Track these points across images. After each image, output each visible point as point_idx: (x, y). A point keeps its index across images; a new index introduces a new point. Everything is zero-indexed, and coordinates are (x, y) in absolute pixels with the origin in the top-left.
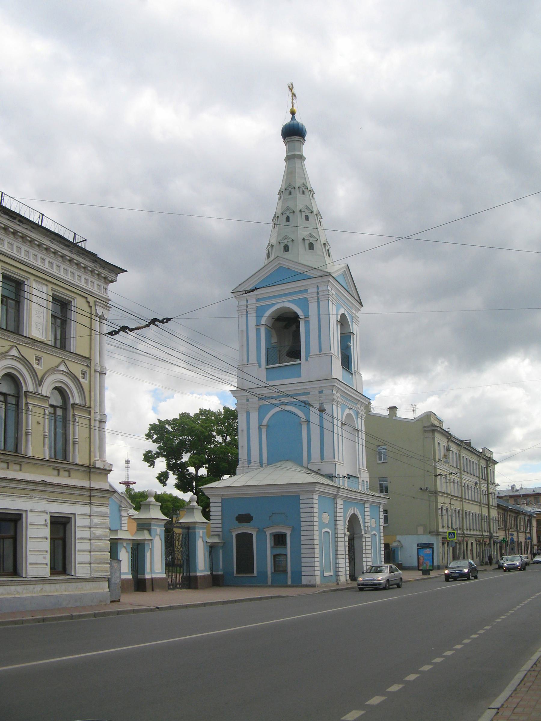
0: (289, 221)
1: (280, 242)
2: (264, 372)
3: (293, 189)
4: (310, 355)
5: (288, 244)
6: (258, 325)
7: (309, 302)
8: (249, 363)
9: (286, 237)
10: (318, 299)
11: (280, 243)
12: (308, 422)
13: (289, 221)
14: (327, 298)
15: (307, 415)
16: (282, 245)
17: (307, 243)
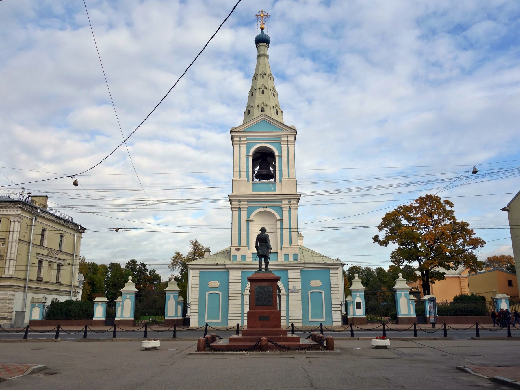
0: (264, 94)
1: (259, 105)
2: (251, 186)
3: (265, 75)
4: (282, 178)
5: (264, 107)
6: (248, 156)
7: (282, 145)
8: (241, 178)
9: (263, 103)
10: (288, 145)
11: (258, 106)
12: (281, 220)
13: (264, 94)
14: (294, 145)
15: (281, 216)
16: (260, 108)
17: (275, 109)
